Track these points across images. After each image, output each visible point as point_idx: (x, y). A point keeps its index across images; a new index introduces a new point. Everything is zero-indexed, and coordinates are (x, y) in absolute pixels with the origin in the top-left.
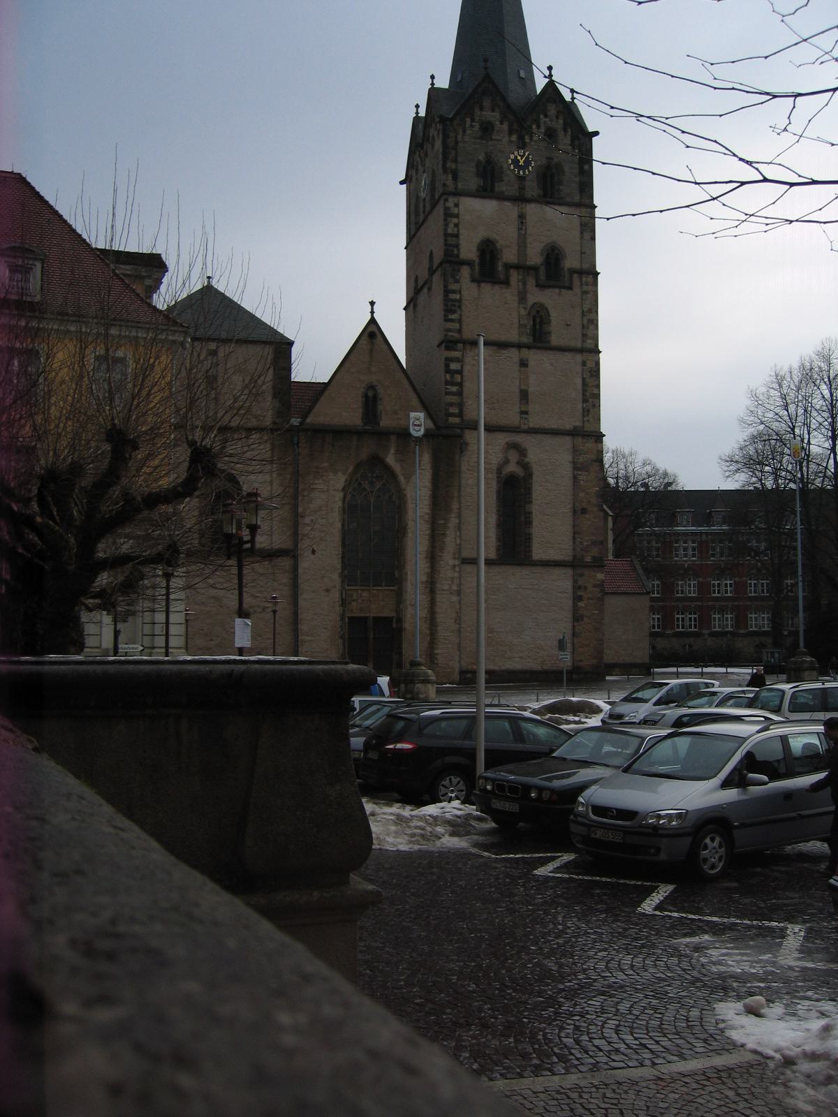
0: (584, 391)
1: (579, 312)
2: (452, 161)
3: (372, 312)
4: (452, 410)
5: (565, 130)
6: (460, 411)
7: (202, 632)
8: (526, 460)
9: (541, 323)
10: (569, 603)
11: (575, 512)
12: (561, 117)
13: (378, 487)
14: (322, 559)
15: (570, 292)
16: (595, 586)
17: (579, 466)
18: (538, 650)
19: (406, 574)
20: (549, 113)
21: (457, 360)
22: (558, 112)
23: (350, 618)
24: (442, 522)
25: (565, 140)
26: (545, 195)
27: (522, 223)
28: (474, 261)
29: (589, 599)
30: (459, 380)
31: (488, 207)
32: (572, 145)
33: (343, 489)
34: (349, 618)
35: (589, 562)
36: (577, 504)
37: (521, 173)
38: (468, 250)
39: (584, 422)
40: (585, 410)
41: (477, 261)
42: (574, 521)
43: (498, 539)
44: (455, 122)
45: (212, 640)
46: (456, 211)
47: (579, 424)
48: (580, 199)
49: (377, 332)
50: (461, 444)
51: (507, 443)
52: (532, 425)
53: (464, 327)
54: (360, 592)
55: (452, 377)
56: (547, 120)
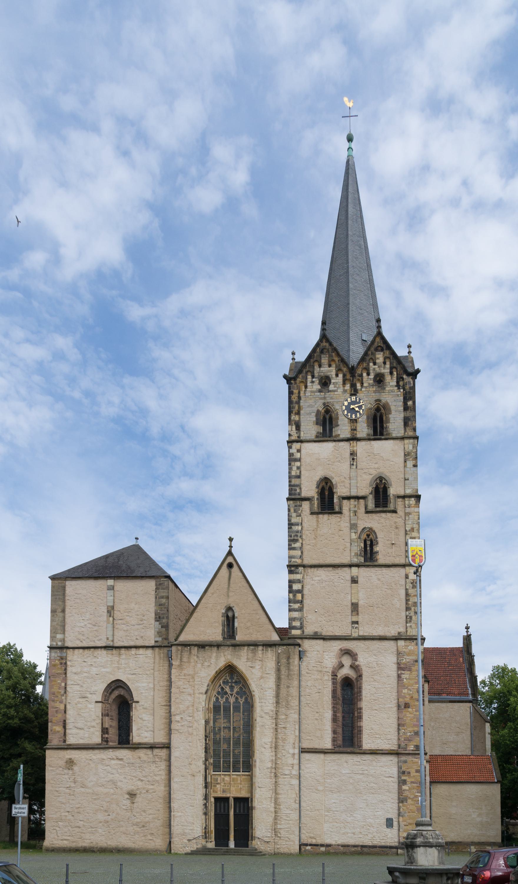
0: (407, 600)
1: (403, 533)
2: (296, 414)
3: (231, 547)
5: (391, 373)
6: (301, 624)
7: (102, 808)
8: (357, 663)
9: (372, 545)
11: (399, 706)
12: (388, 363)
14: (190, 748)
15: (394, 515)
17: (402, 666)
18: (368, 827)
20: (377, 361)
21: (299, 581)
22: (385, 358)
24: (283, 717)
25: (391, 382)
26: (375, 433)
27: (353, 459)
28: (314, 497)
29: (412, 782)
30: (300, 598)
31: (327, 448)
32: (398, 385)
33: (206, 693)
35: (412, 750)
36: (401, 700)
37: (354, 416)
38: (309, 488)
39: (407, 628)
40: (408, 617)
41: (316, 496)
42: (398, 714)
43: (334, 732)
44: (298, 380)
45: (109, 815)
46: (298, 455)
47: (402, 630)
48: (405, 433)
49: (234, 563)
50: (300, 651)
51: (341, 650)
52: (361, 634)
53: (305, 553)
54: (222, 776)
55: (294, 596)
56: (376, 367)
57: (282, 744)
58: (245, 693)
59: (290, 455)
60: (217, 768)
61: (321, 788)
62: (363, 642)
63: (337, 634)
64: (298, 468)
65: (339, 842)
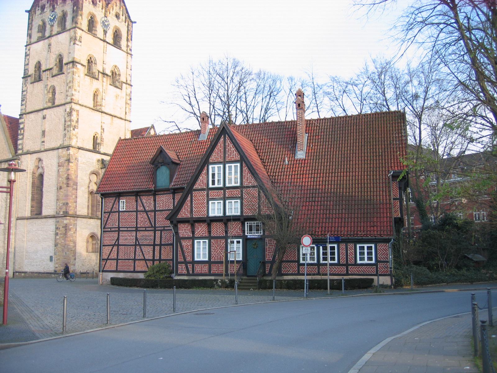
10: (53, 236)
16: (63, 227)
29: (61, 234)
39: (64, 141)
43: (32, 207)
52: (45, 148)
59: (26, 53)
62: (45, 152)
64: (28, 59)
65: (31, 271)
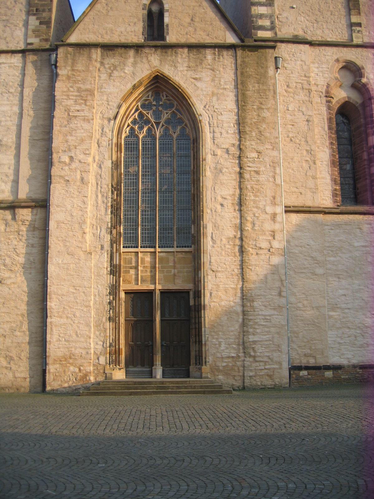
4: (260, 23)
8: (364, 80)
13: (166, 116)
19: (205, 227)
23: (127, 293)
34: (127, 293)
57: (253, 198)
58: (180, 121)
60: (132, 241)
61: (320, 271)
63: (329, 40)
65: (355, 361)
